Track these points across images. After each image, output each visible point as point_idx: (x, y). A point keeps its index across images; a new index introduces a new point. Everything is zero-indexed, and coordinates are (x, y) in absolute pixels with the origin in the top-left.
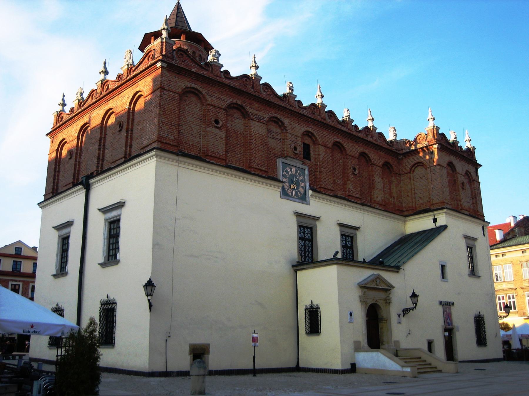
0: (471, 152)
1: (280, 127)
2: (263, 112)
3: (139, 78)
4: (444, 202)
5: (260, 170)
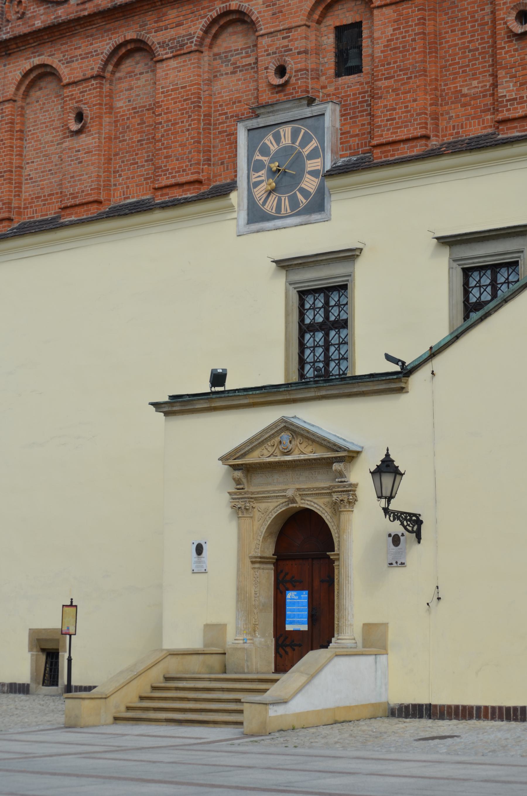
2: (192, 21)
5: (177, 187)
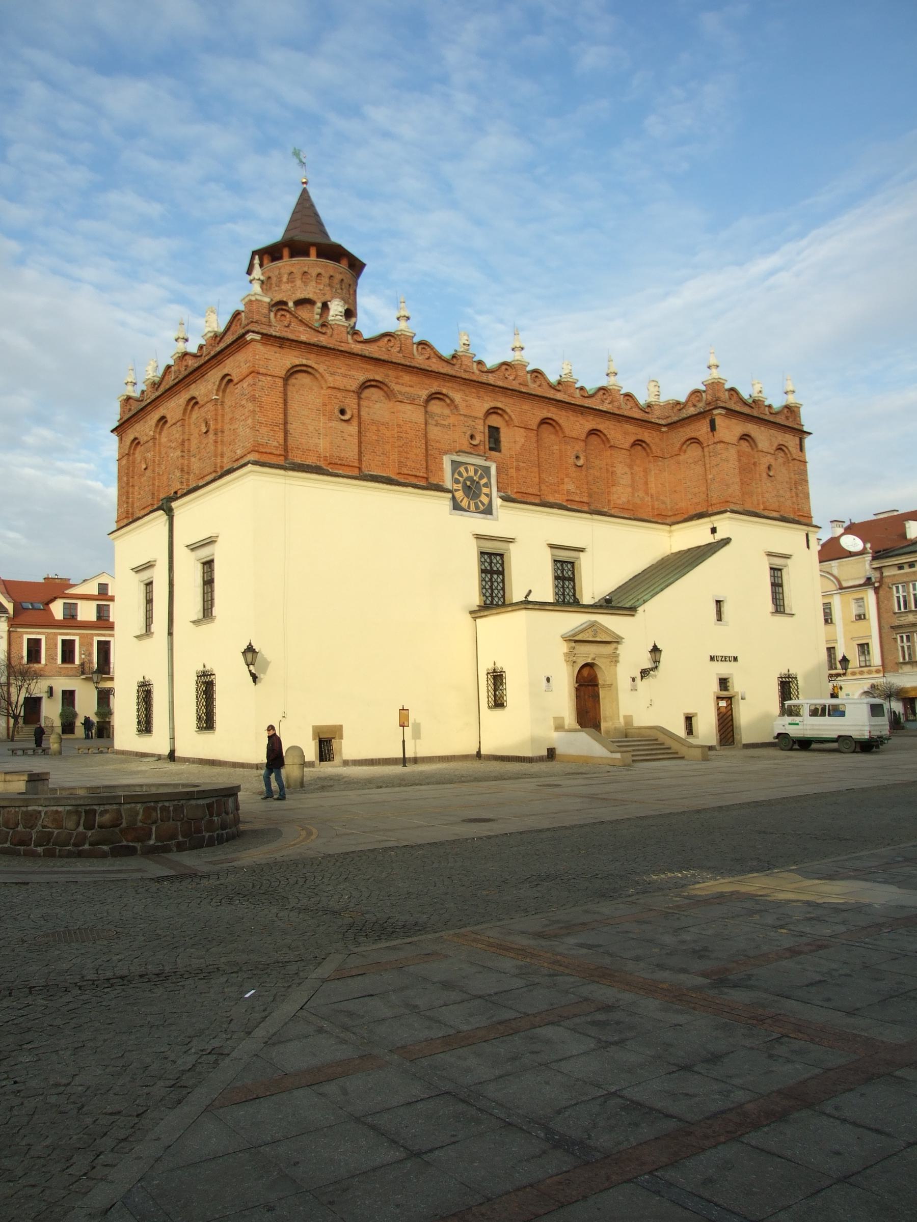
0: (791, 410)
1: (448, 405)
3: (225, 355)
4: (727, 502)
